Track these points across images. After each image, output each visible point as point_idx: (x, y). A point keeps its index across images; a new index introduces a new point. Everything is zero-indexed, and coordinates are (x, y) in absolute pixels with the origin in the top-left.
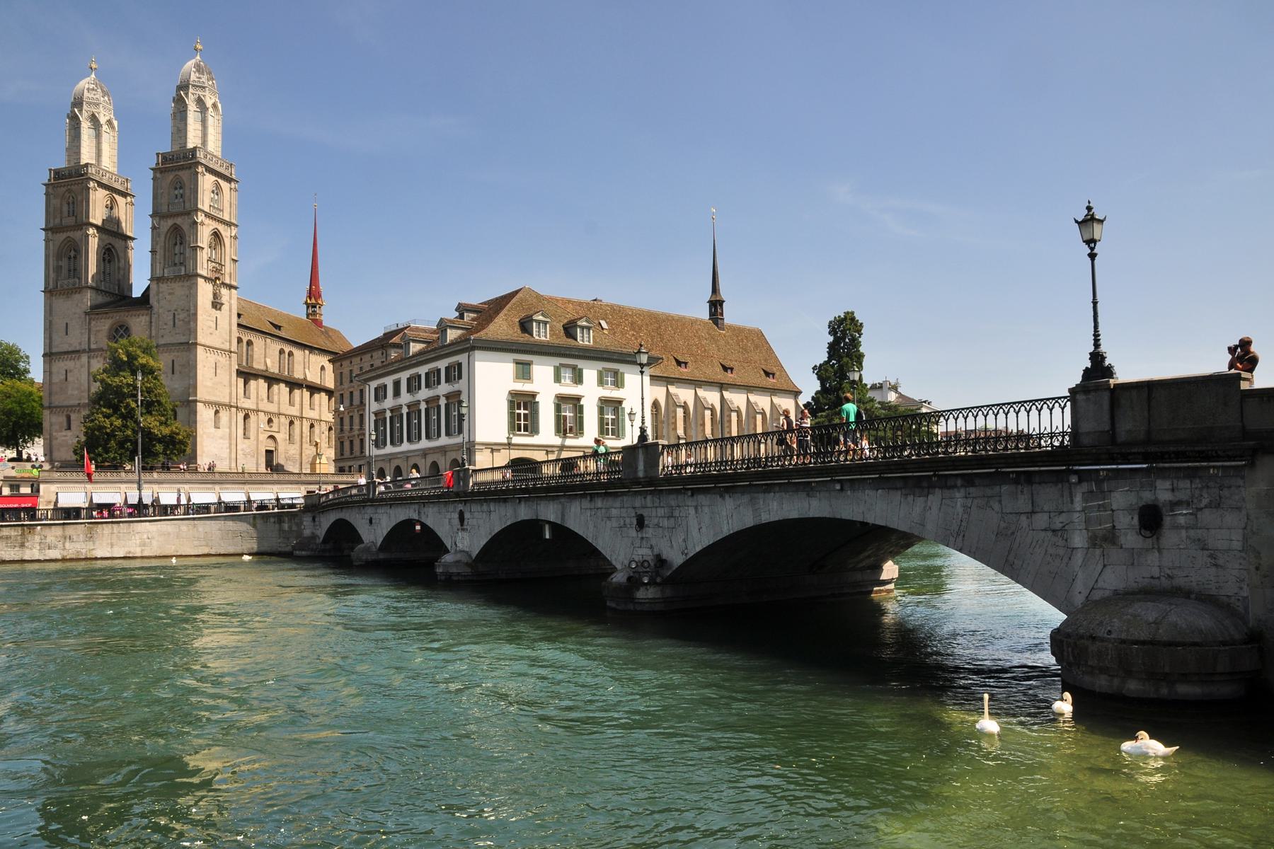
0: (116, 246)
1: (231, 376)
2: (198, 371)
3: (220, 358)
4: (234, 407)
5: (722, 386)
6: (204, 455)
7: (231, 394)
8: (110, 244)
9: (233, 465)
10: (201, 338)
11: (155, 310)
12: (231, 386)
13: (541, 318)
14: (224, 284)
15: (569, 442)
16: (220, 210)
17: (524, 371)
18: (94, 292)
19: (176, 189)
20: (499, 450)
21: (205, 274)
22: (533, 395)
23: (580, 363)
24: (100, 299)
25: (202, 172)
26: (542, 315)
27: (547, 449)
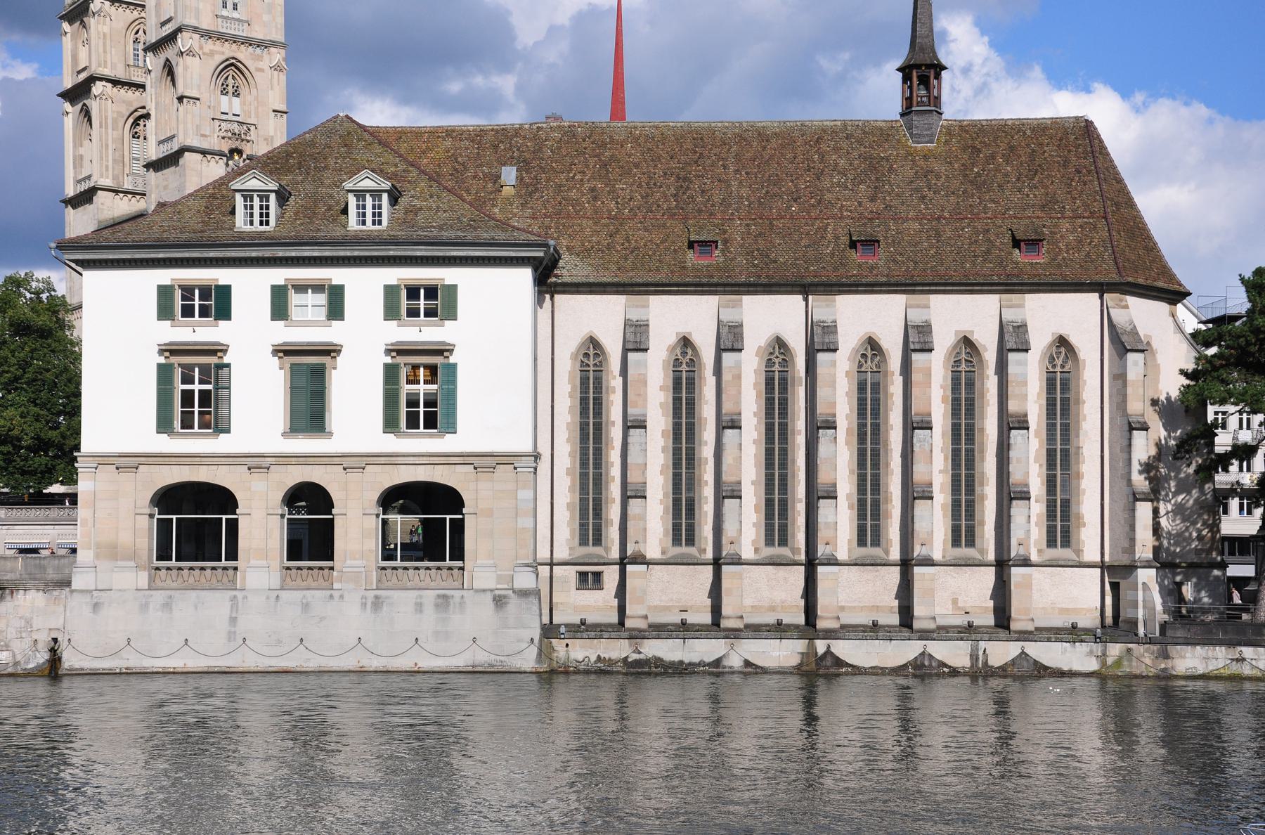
5: (805, 289)
21: (205, 145)
23: (335, 275)
27: (256, 463)
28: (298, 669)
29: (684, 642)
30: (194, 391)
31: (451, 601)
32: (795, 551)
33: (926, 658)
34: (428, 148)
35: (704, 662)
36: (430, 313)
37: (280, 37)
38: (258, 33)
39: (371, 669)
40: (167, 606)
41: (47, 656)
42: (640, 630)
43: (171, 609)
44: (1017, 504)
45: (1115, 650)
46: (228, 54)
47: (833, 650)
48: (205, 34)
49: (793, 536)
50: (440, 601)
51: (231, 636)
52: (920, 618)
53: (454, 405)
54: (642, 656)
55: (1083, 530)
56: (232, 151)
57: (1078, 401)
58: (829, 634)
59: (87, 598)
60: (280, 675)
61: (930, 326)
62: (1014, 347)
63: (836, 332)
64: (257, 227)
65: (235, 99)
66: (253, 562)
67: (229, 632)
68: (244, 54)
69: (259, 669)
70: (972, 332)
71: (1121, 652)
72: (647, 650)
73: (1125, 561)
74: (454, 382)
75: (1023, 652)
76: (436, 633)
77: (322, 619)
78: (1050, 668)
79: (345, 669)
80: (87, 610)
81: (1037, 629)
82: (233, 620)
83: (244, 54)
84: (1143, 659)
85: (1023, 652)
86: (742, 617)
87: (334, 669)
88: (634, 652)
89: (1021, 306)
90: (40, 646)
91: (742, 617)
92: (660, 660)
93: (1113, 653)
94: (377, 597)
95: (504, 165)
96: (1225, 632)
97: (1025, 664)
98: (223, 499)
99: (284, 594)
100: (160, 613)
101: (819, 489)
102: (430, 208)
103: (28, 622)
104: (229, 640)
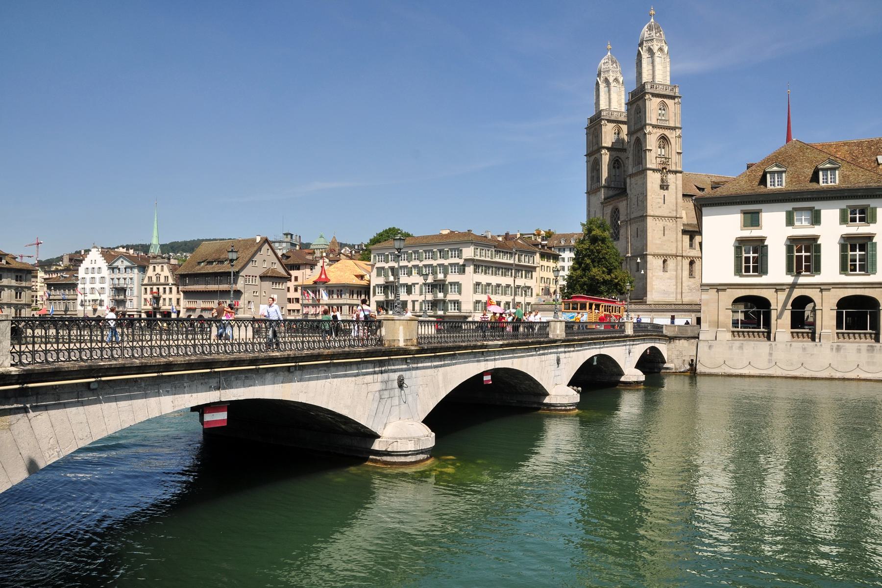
0: (622, 157)
1: (677, 234)
2: (648, 234)
3: (667, 223)
4: (680, 256)
6: (653, 291)
7: (677, 247)
8: (618, 157)
9: (679, 297)
10: (650, 212)
11: (629, 195)
12: (677, 241)
13: (775, 169)
14: (670, 171)
15: (802, 280)
16: (667, 120)
17: (753, 220)
18: (606, 189)
19: (660, 109)
20: (725, 290)
21: (654, 167)
22: (762, 240)
23: (816, 205)
24: (611, 193)
25: (649, 98)
26: (777, 166)
27: (778, 287)
28: (802, 376)
30: (750, 257)
31: (875, 348)
34: (837, 151)
36: (862, 219)
37: (678, 125)
38: (672, 124)
39: (837, 377)
40: (741, 348)
41: (688, 367)
43: (743, 349)
46: (662, 132)
48: (654, 126)
50: (869, 348)
51: (770, 361)
53: (876, 261)
56: (663, 168)
59: (706, 344)
60: (789, 380)
64: (777, 187)
65: (663, 150)
66: (778, 330)
67: (769, 359)
68: (667, 133)
69: (784, 375)
74: (875, 251)
76: (868, 363)
77: (812, 355)
79: (824, 376)
80: (706, 349)
82: (771, 354)
83: (667, 133)
87: (818, 376)
90: (686, 362)
94: (838, 346)
95: (877, 155)
98: (762, 304)
99: (794, 344)
100: (738, 351)
102: (854, 175)
103: (681, 352)
104: (769, 362)
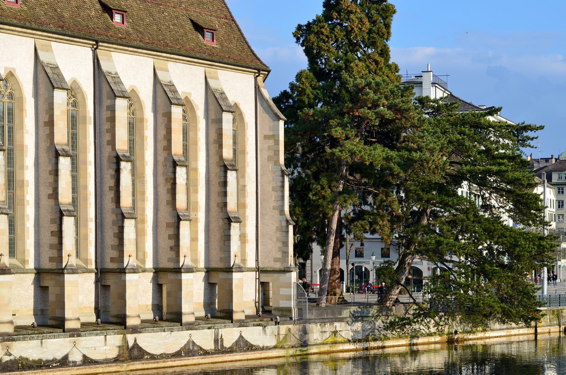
29: (42, 343)
32: (86, 261)
33: (191, 344)
35: (56, 359)
42: (9, 335)
44: (234, 227)
45: (283, 329)
47: (138, 342)
49: (86, 249)
52: (185, 314)
54: (12, 358)
55: (247, 245)
57: (244, 152)
58: (135, 330)
61: (173, 85)
62: (227, 109)
63: (121, 83)
70: (190, 94)
71: (286, 332)
72: (16, 351)
73: (278, 266)
75: (241, 337)
78: (255, 346)
81: (247, 317)
84: (295, 336)
85: (241, 337)
86: (78, 319)
88: (6, 354)
89: (216, 78)
91: (78, 319)
92: (27, 359)
93: (283, 333)
96: (327, 314)
97: (242, 344)
101: (124, 211)
